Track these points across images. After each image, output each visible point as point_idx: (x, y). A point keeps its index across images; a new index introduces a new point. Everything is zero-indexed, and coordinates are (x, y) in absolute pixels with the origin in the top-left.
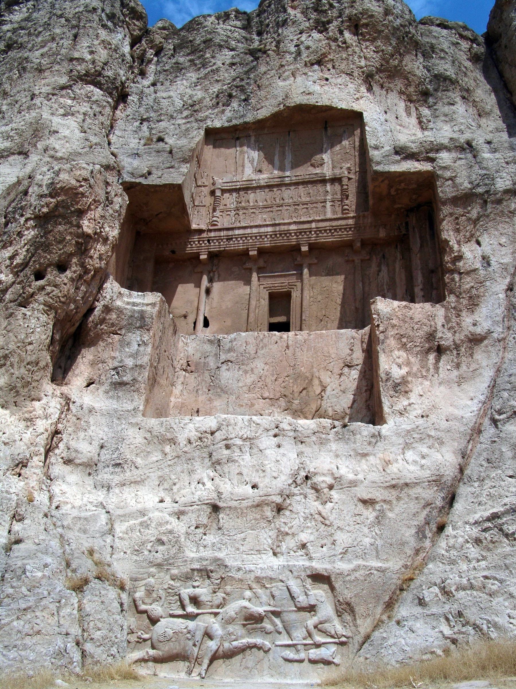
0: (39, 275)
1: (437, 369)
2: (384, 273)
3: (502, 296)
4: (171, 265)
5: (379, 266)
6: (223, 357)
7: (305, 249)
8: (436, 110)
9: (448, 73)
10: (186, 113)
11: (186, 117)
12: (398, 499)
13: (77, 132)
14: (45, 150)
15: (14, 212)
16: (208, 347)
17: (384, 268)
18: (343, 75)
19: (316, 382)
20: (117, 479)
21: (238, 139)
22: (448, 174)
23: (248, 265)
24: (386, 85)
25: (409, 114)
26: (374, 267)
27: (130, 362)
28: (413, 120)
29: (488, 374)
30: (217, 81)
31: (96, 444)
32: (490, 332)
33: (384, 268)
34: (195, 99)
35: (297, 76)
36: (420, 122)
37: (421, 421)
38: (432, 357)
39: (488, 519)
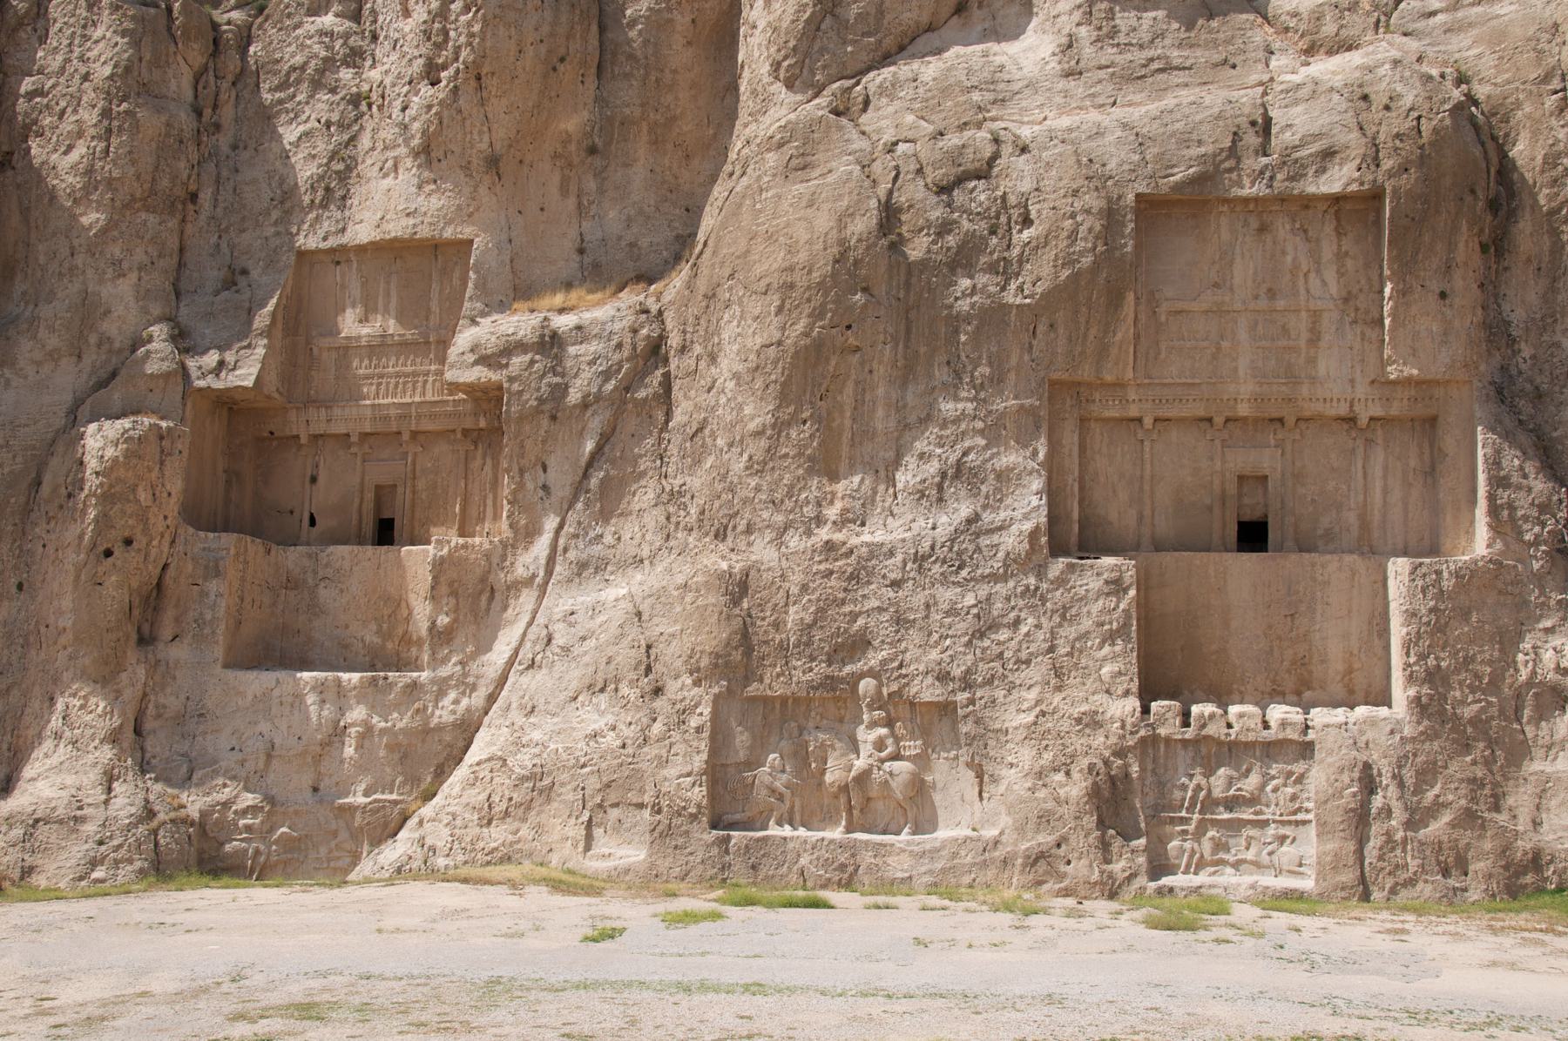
0: (108, 553)
1: (488, 610)
2: (488, 468)
3: (551, 535)
4: (275, 443)
5: (484, 458)
6: (321, 574)
7: (406, 437)
8: (604, 179)
9: (627, 111)
10: (275, 214)
11: (276, 223)
12: (423, 741)
13: (132, 304)
14: (99, 346)
15: (73, 484)
16: (306, 562)
17: (489, 461)
18: (458, 171)
19: (403, 604)
20: (202, 728)
21: (338, 263)
22: (516, 387)
23: (354, 449)
24: (528, 158)
25: (564, 191)
26: (478, 462)
27: (208, 617)
28: (571, 202)
29: (526, 618)
30: (314, 157)
31: (182, 697)
32: (534, 576)
33: (489, 461)
34: (285, 187)
35: (400, 171)
36: (580, 204)
37: (459, 668)
38: (484, 598)
39: (478, 764)
